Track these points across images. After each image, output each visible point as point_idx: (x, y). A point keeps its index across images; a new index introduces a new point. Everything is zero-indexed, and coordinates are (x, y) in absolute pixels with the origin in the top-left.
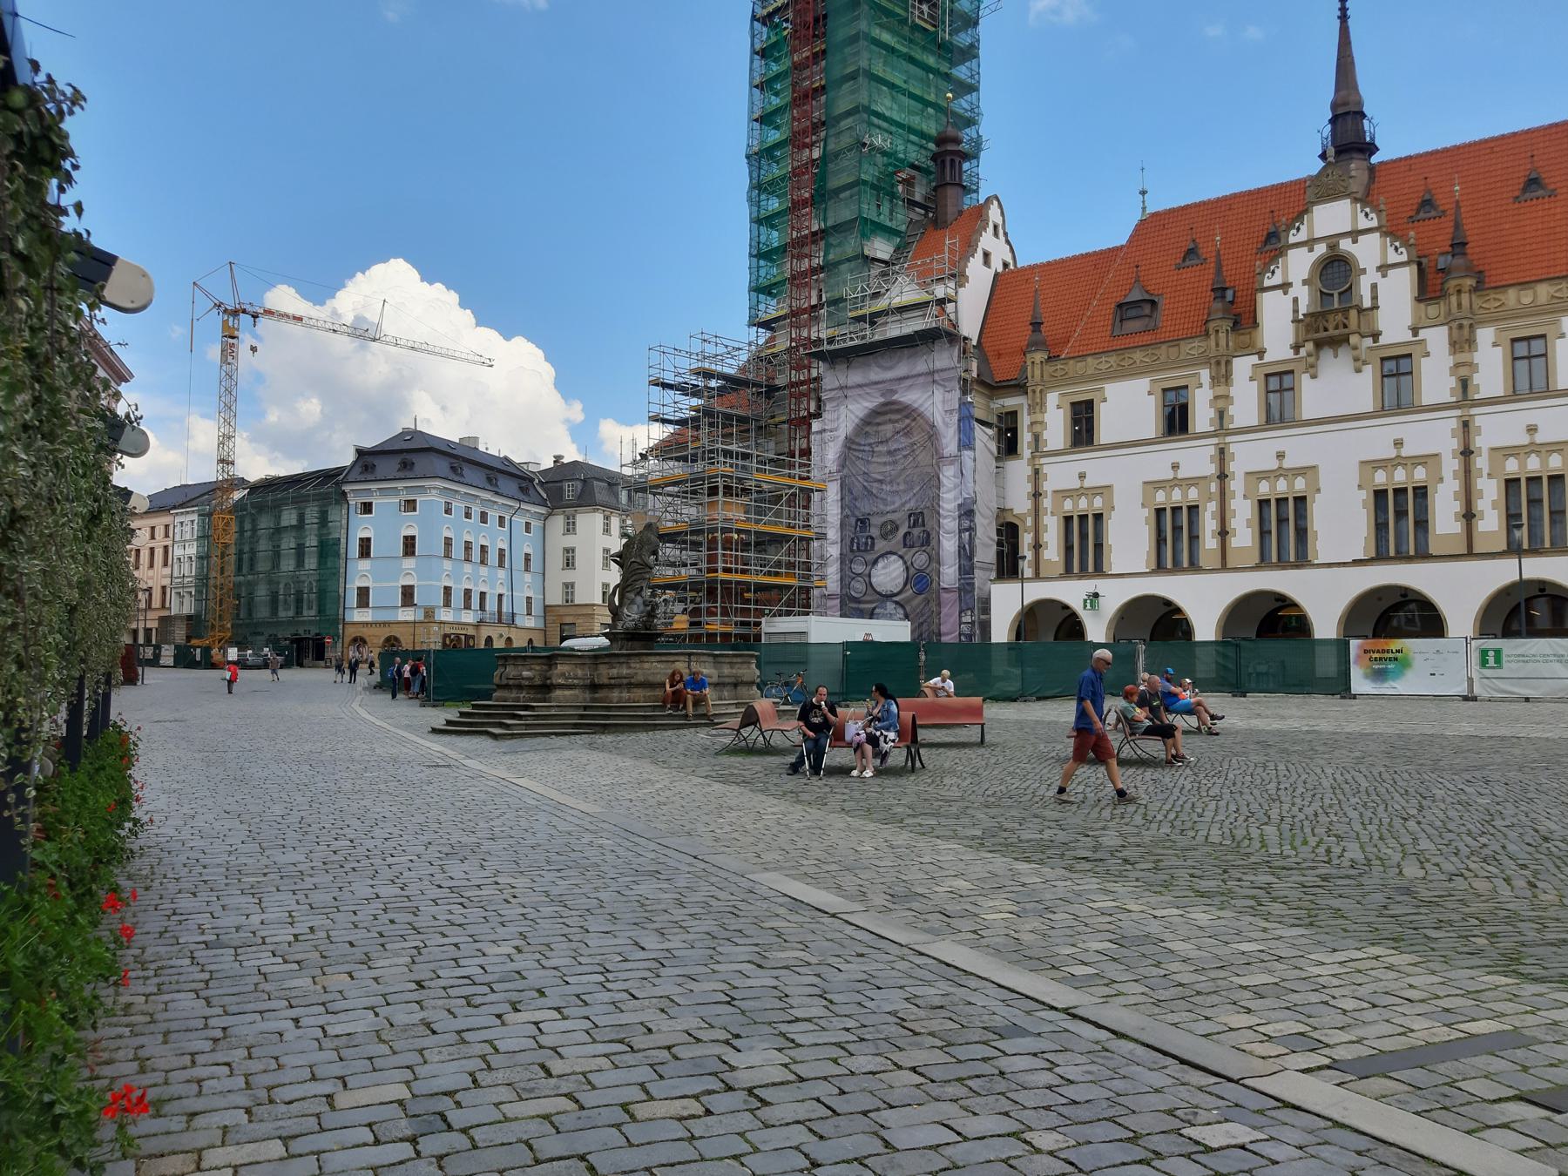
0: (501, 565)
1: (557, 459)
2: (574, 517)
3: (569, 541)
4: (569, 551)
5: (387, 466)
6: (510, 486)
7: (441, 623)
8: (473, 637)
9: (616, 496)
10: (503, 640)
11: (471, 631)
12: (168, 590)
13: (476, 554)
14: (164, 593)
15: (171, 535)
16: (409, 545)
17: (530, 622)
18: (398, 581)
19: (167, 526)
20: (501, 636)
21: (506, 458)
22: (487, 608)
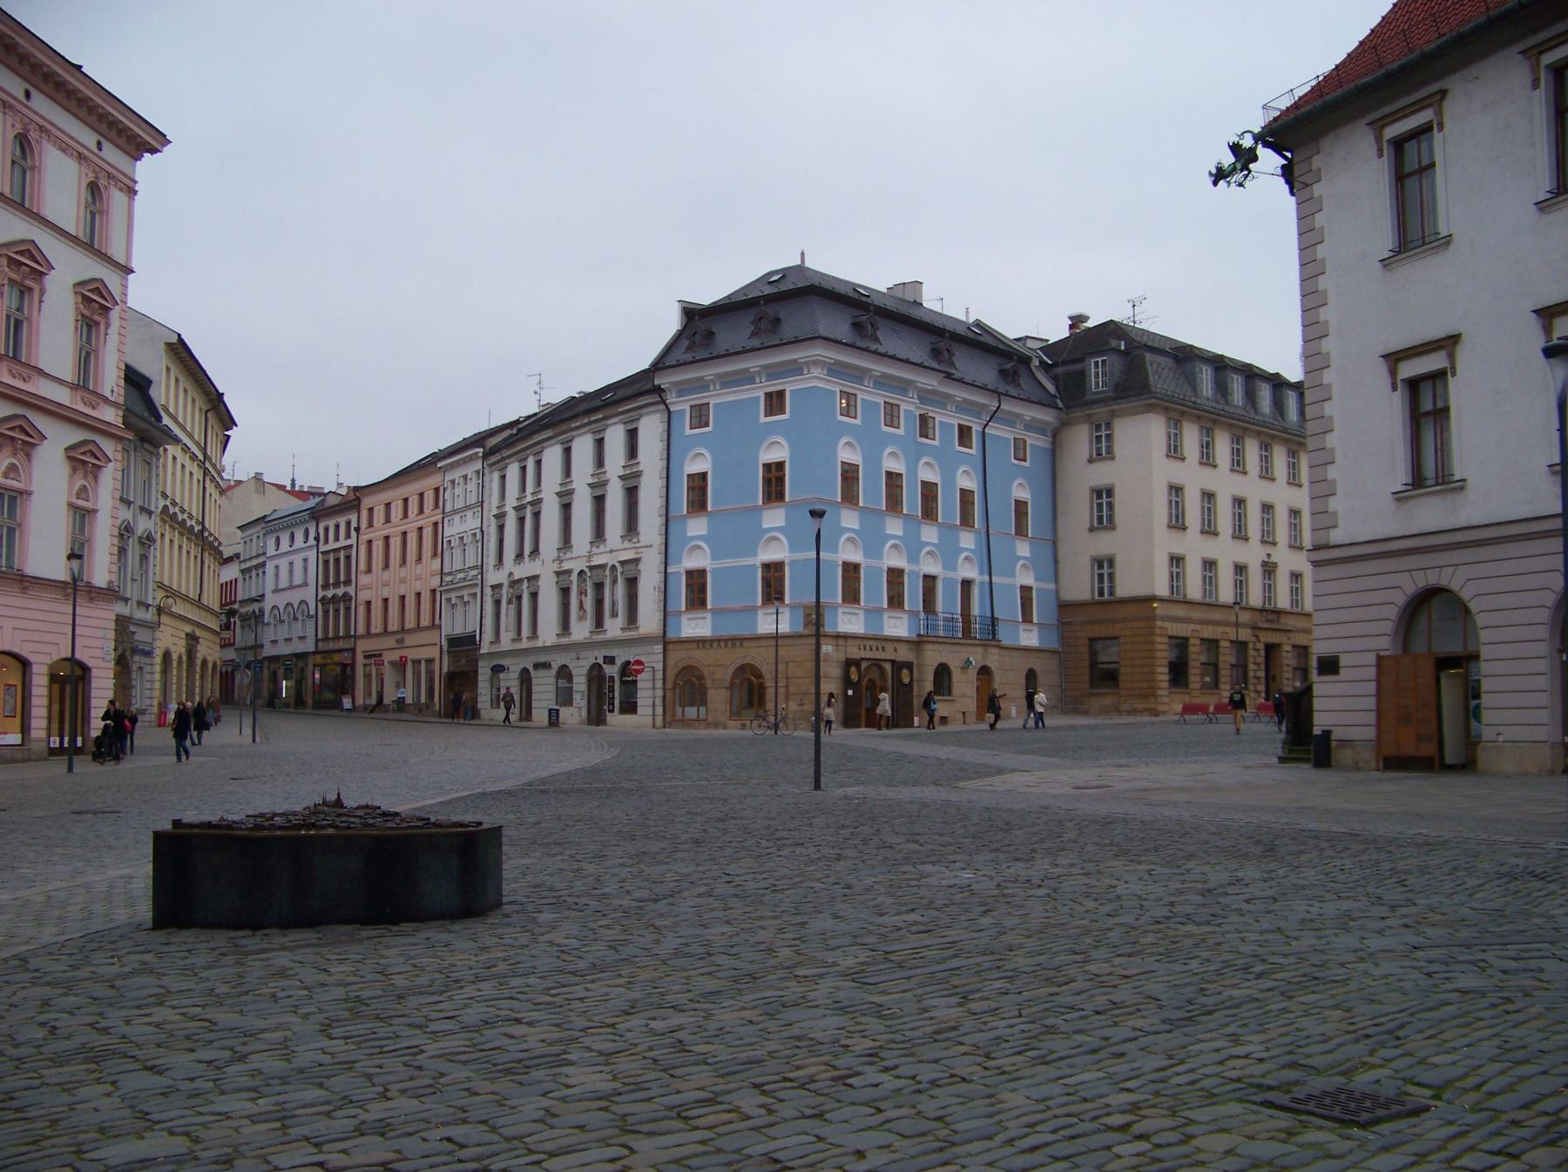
0: (967, 521)
1: (1076, 320)
2: (1109, 425)
3: (1102, 474)
4: (1103, 495)
5: (731, 334)
6: (985, 372)
7: (845, 637)
8: (909, 666)
9: (1192, 382)
10: (972, 674)
11: (904, 654)
12: (438, 594)
13: (911, 500)
14: (434, 600)
15: (441, 505)
16: (774, 479)
17: (1030, 638)
18: (755, 554)
19: (437, 490)
20: (968, 662)
21: (978, 324)
22: (939, 607)
